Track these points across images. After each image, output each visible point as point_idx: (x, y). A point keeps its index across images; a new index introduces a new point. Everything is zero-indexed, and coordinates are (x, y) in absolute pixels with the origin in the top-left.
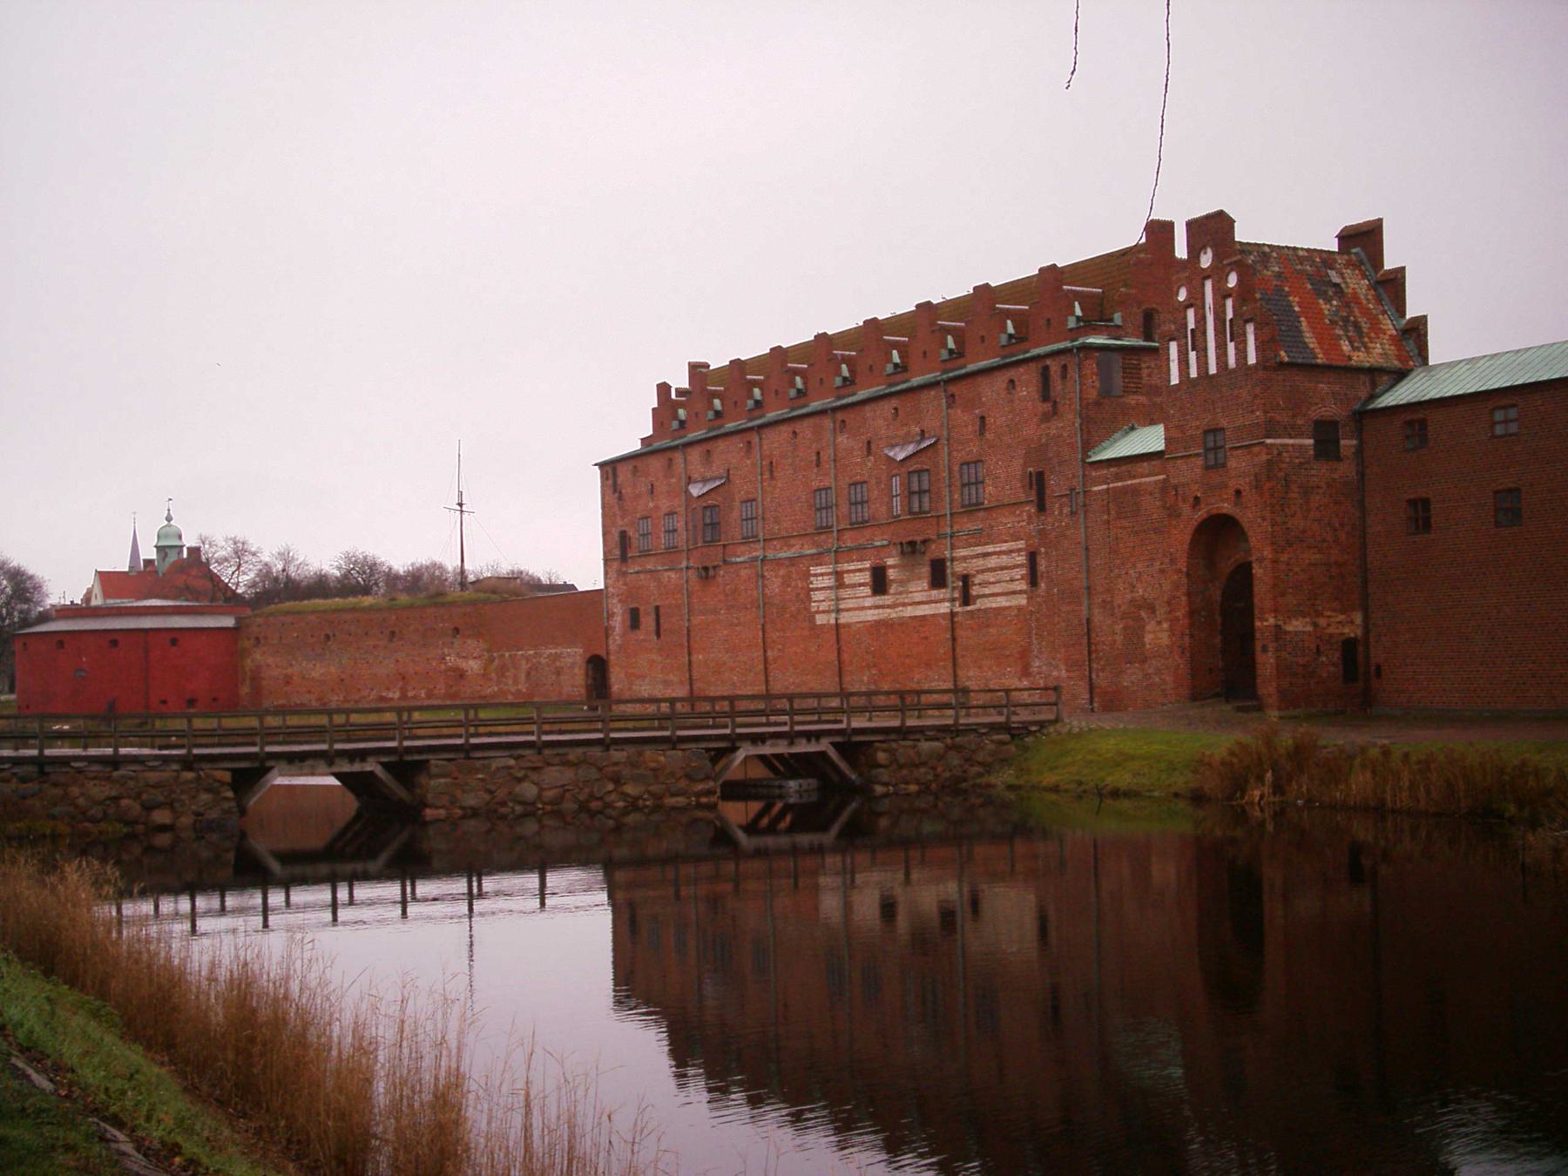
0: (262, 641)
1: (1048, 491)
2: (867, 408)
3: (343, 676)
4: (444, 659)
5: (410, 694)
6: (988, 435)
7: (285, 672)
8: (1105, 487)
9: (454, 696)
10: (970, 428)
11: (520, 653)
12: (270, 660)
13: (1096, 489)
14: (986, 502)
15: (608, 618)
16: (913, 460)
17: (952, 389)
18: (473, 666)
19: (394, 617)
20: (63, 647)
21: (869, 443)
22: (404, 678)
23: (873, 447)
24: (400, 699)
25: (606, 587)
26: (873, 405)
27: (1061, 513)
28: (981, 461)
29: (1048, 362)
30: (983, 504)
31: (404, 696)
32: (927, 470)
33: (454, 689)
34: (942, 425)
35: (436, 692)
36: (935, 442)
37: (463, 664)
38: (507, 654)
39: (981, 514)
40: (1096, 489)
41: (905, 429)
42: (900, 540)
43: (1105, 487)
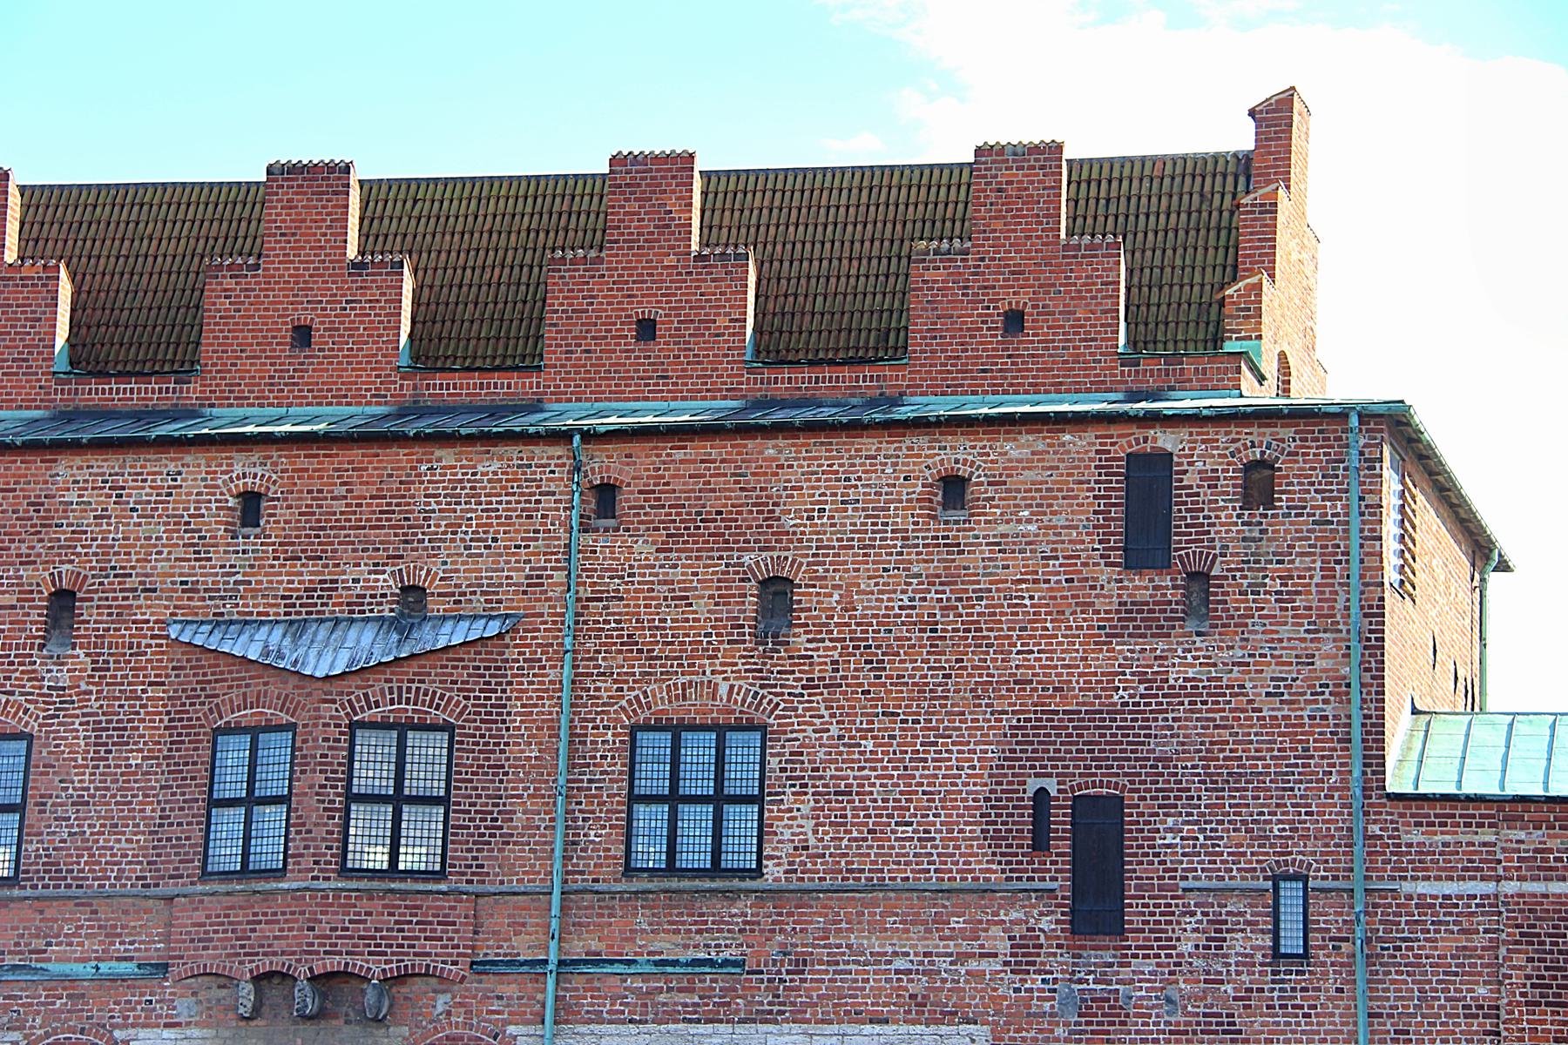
1: (1137, 870)
2: (66, 469)
6: (800, 641)
8: (1489, 888)
10: (702, 607)
13: (1422, 888)
14: (773, 872)
16: (378, 685)
17: (604, 464)
21: (63, 602)
23: (90, 614)
26: (105, 464)
27: (1215, 942)
28: (763, 728)
29: (1166, 440)
30: (758, 872)
32: (447, 727)
34: (535, 581)
36: (500, 636)
39: (744, 906)
40: (1422, 888)
41: (308, 573)
42: (265, 964)
43: (1489, 888)
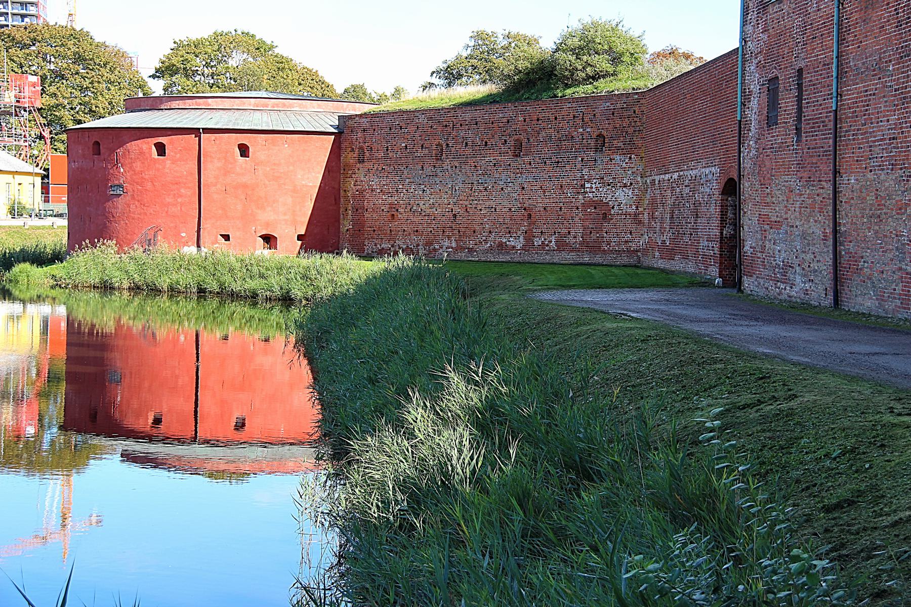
0: (367, 154)
3: (457, 210)
4: (583, 186)
5: (537, 242)
7: (390, 200)
9: (594, 248)
11: (667, 176)
12: (375, 183)
15: (743, 104)
18: (623, 196)
19: (521, 119)
20: (99, 154)
22: (530, 216)
24: (524, 248)
25: (744, 40)
31: (529, 245)
33: (594, 236)
35: (570, 240)
37: (605, 194)
38: (657, 178)
